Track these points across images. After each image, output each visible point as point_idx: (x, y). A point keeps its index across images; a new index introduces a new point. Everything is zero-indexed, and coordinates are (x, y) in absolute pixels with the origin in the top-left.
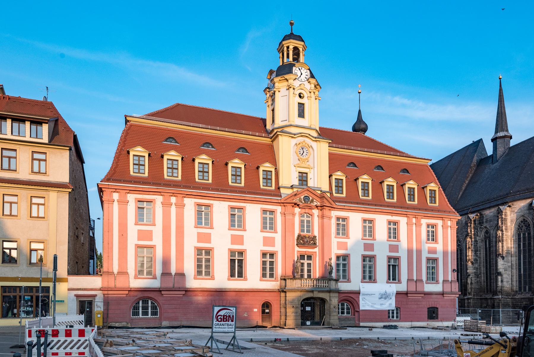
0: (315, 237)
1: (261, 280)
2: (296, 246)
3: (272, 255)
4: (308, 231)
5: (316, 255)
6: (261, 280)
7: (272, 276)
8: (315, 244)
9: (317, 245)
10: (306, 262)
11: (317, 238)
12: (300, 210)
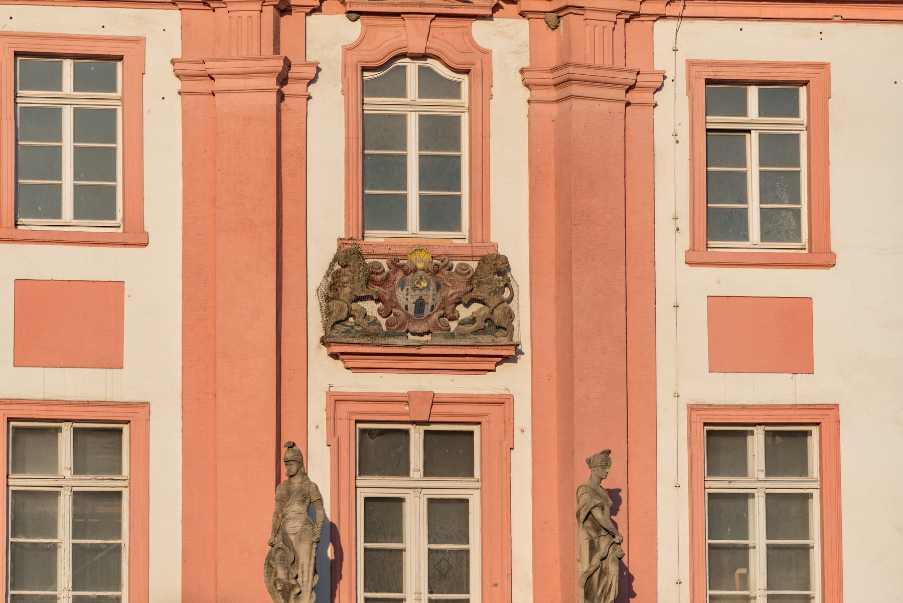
0: (498, 267)
2: (319, 356)
5: (509, 422)
8: (498, 324)
9: (523, 330)
10: (416, 492)
11: (520, 273)
12: (354, 30)
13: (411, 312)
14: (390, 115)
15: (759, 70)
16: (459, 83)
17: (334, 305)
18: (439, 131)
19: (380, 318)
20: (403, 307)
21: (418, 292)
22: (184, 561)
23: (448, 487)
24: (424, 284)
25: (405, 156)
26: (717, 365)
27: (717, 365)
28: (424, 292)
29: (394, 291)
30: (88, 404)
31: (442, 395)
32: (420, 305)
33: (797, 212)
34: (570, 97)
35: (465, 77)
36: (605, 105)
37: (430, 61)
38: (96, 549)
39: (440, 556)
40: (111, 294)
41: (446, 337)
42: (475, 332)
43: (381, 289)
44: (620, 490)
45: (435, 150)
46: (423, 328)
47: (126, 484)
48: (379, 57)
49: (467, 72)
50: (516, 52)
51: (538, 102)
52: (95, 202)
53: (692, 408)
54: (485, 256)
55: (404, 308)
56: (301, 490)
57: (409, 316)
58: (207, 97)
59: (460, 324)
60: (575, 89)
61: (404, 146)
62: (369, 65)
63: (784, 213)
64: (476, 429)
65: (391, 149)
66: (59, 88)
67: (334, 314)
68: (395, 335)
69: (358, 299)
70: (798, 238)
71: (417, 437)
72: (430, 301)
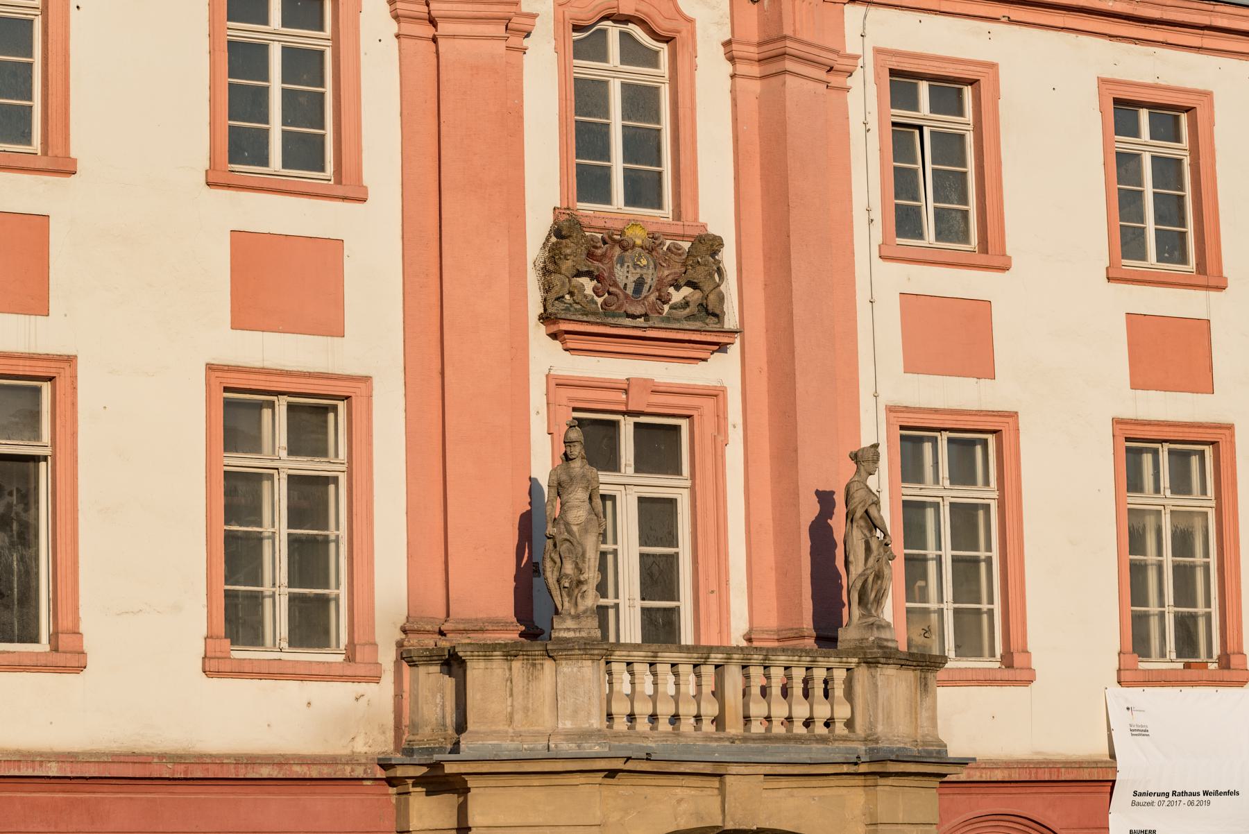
1: (213, 667)
3: (312, 416)
4: (643, 190)
5: (721, 417)
6: (213, 667)
7: (310, 623)
8: (710, 311)
11: (728, 257)
13: (629, 291)
14: (593, 80)
15: (936, 64)
16: (657, 53)
17: (556, 279)
18: (640, 101)
19: (596, 298)
20: (622, 286)
21: (638, 270)
22: (410, 556)
23: (658, 485)
24: (644, 262)
25: (608, 125)
26: (911, 366)
27: (911, 366)
29: (612, 268)
30: (310, 375)
31: (659, 385)
32: (639, 284)
33: (965, 214)
34: (785, 72)
35: (664, 46)
36: (811, 85)
37: (631, 26)
38: (313, 540)
39: (652, 559)
40: (328, 252)
41: (663, 320)
42: (688, 318)
44: (833, 493)
45: (637, 120)
46: (638, 310)
47: (344, 468)
48: (591, 14)
49: (668, 40)
50: (717, 23)
51: (744, 76)
52: (304, 153)
53: (891, 409)
54: (700, 236)
56: (584, 476)
57: (627, 296)
58: (425, 43)
59: (671, 308)
60: (789, 65)
61: (606, 114)
62: (580, 23)
63: (954, 214)
64: (684, 424)
65: (595, 116)
66: (265, 21)
67: (556, 289)
68: (606, 315)
69: (579, 274)
70: (966, 240)
71: (627, 429)
72: (649, 281)
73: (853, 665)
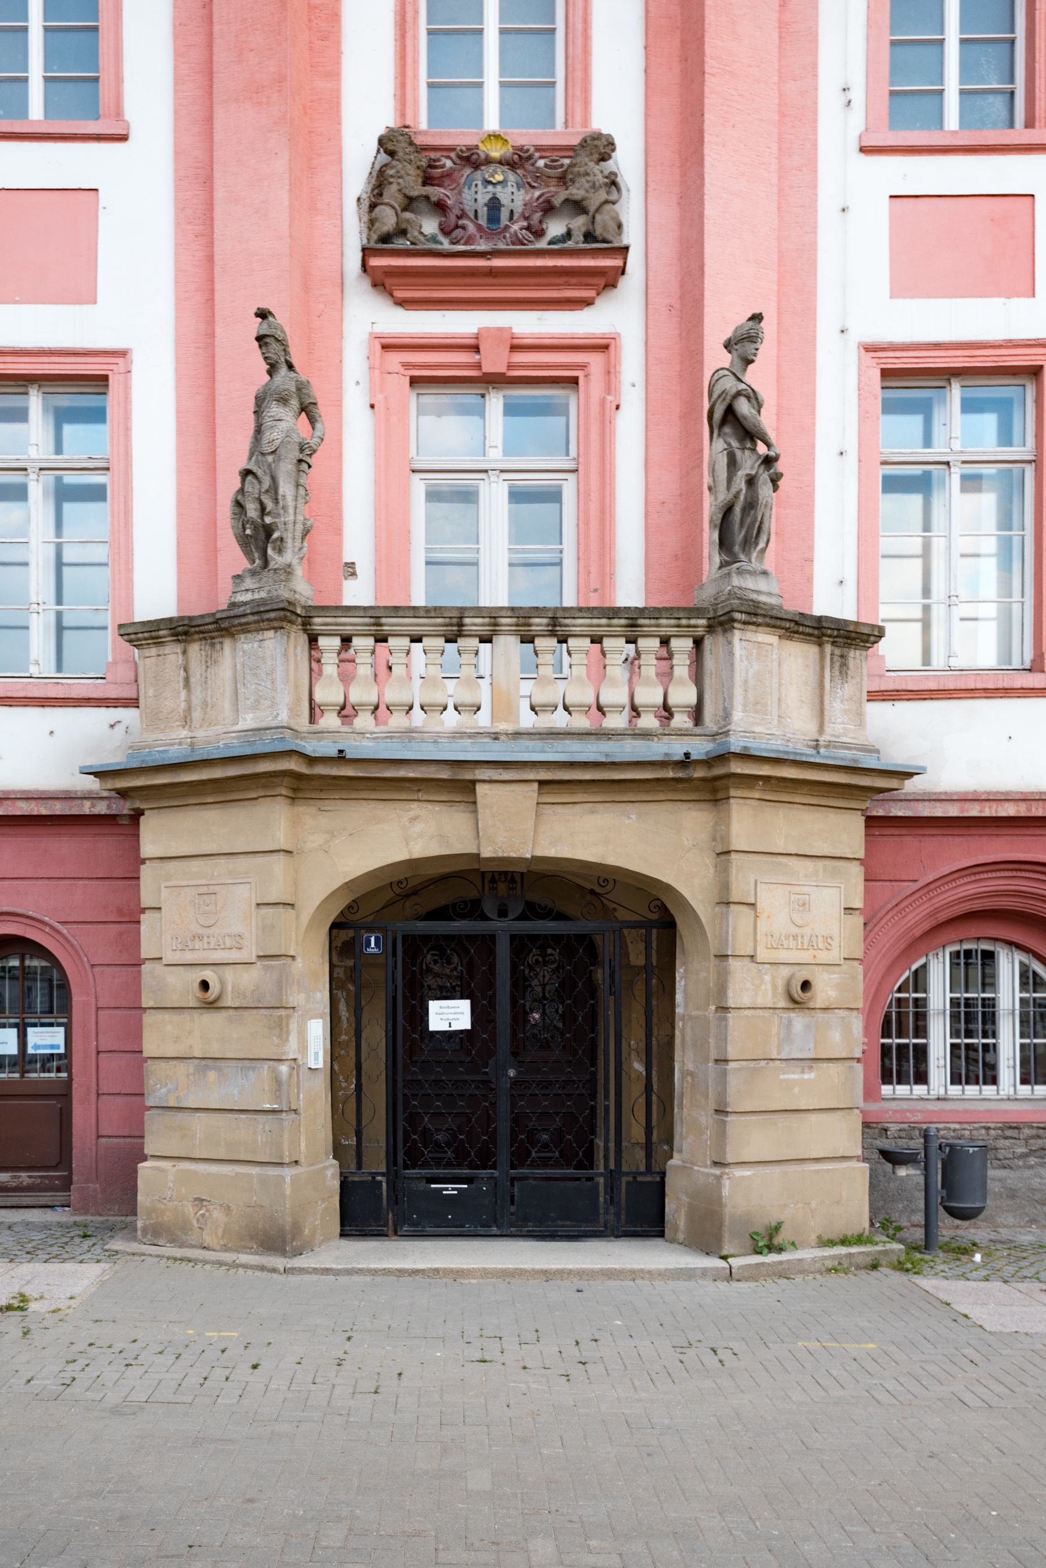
13: (483, 221)
21: (490, 188)
24: (499, 177)
28: (499, 188)
43: (442, 190)
55: (472, 216)
57: (479, 228)
73: (700, 631)
